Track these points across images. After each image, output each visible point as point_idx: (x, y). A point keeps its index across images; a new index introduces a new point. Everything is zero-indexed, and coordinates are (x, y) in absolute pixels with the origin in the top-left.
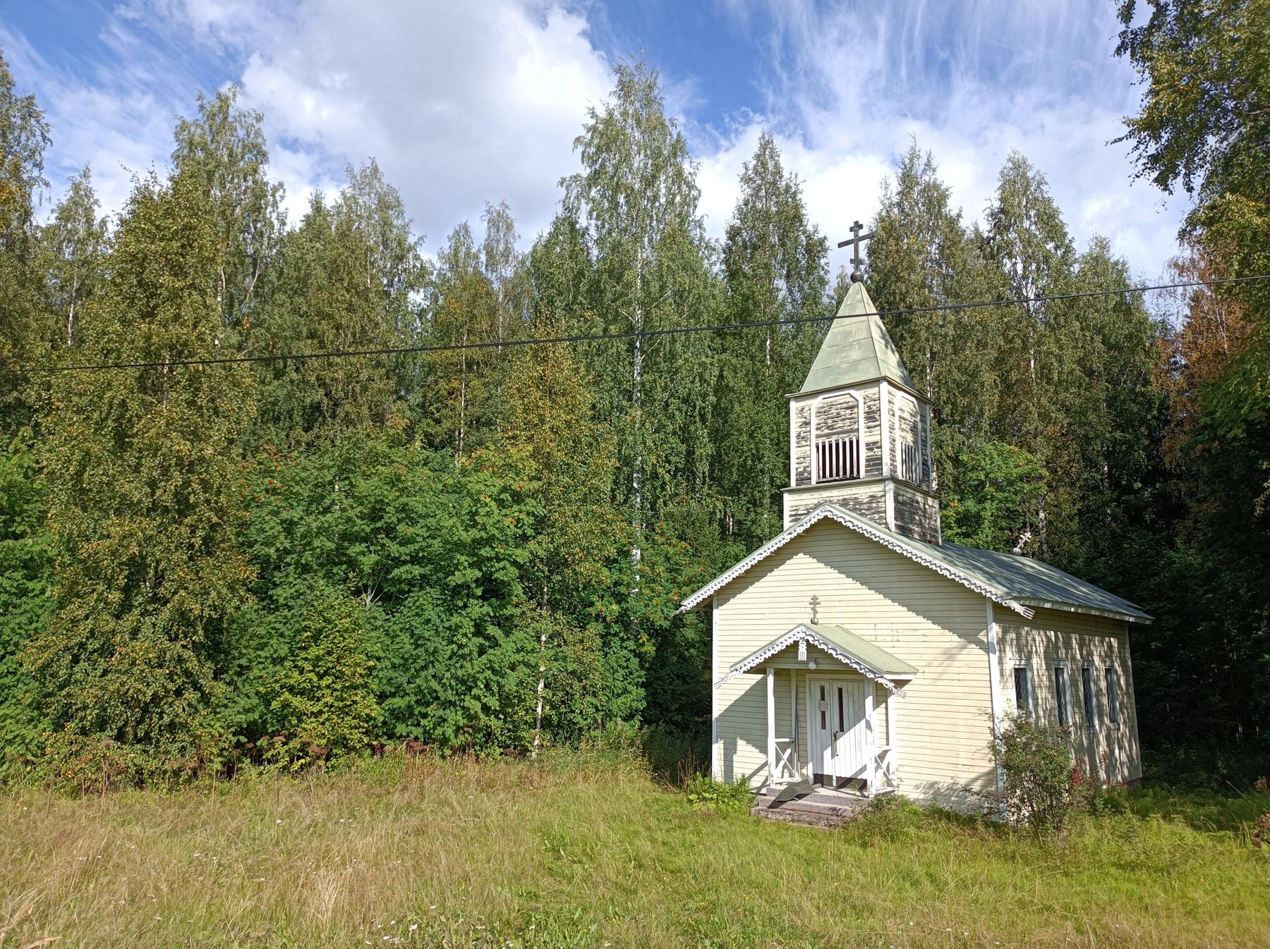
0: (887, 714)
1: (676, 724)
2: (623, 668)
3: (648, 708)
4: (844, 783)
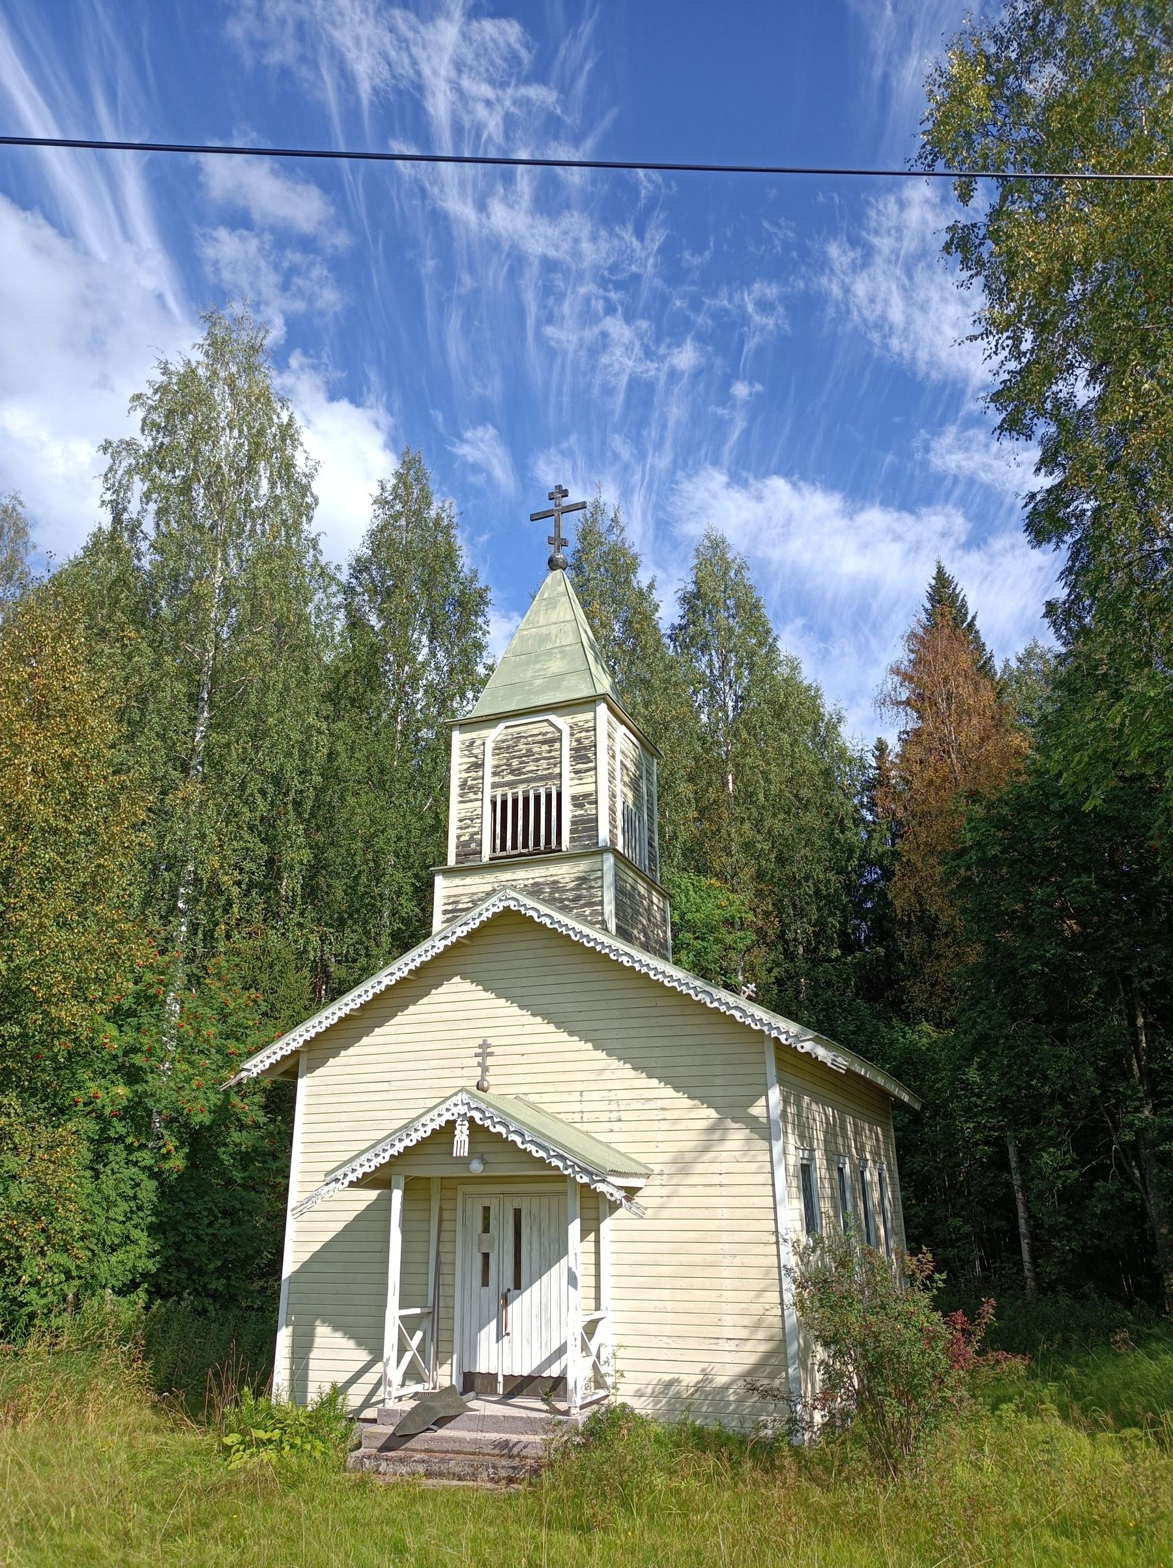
0: (597, 1253)
1: (215, 1296)
2: (127, 1198)
3: (165, 1268)
4: (519, 1386)
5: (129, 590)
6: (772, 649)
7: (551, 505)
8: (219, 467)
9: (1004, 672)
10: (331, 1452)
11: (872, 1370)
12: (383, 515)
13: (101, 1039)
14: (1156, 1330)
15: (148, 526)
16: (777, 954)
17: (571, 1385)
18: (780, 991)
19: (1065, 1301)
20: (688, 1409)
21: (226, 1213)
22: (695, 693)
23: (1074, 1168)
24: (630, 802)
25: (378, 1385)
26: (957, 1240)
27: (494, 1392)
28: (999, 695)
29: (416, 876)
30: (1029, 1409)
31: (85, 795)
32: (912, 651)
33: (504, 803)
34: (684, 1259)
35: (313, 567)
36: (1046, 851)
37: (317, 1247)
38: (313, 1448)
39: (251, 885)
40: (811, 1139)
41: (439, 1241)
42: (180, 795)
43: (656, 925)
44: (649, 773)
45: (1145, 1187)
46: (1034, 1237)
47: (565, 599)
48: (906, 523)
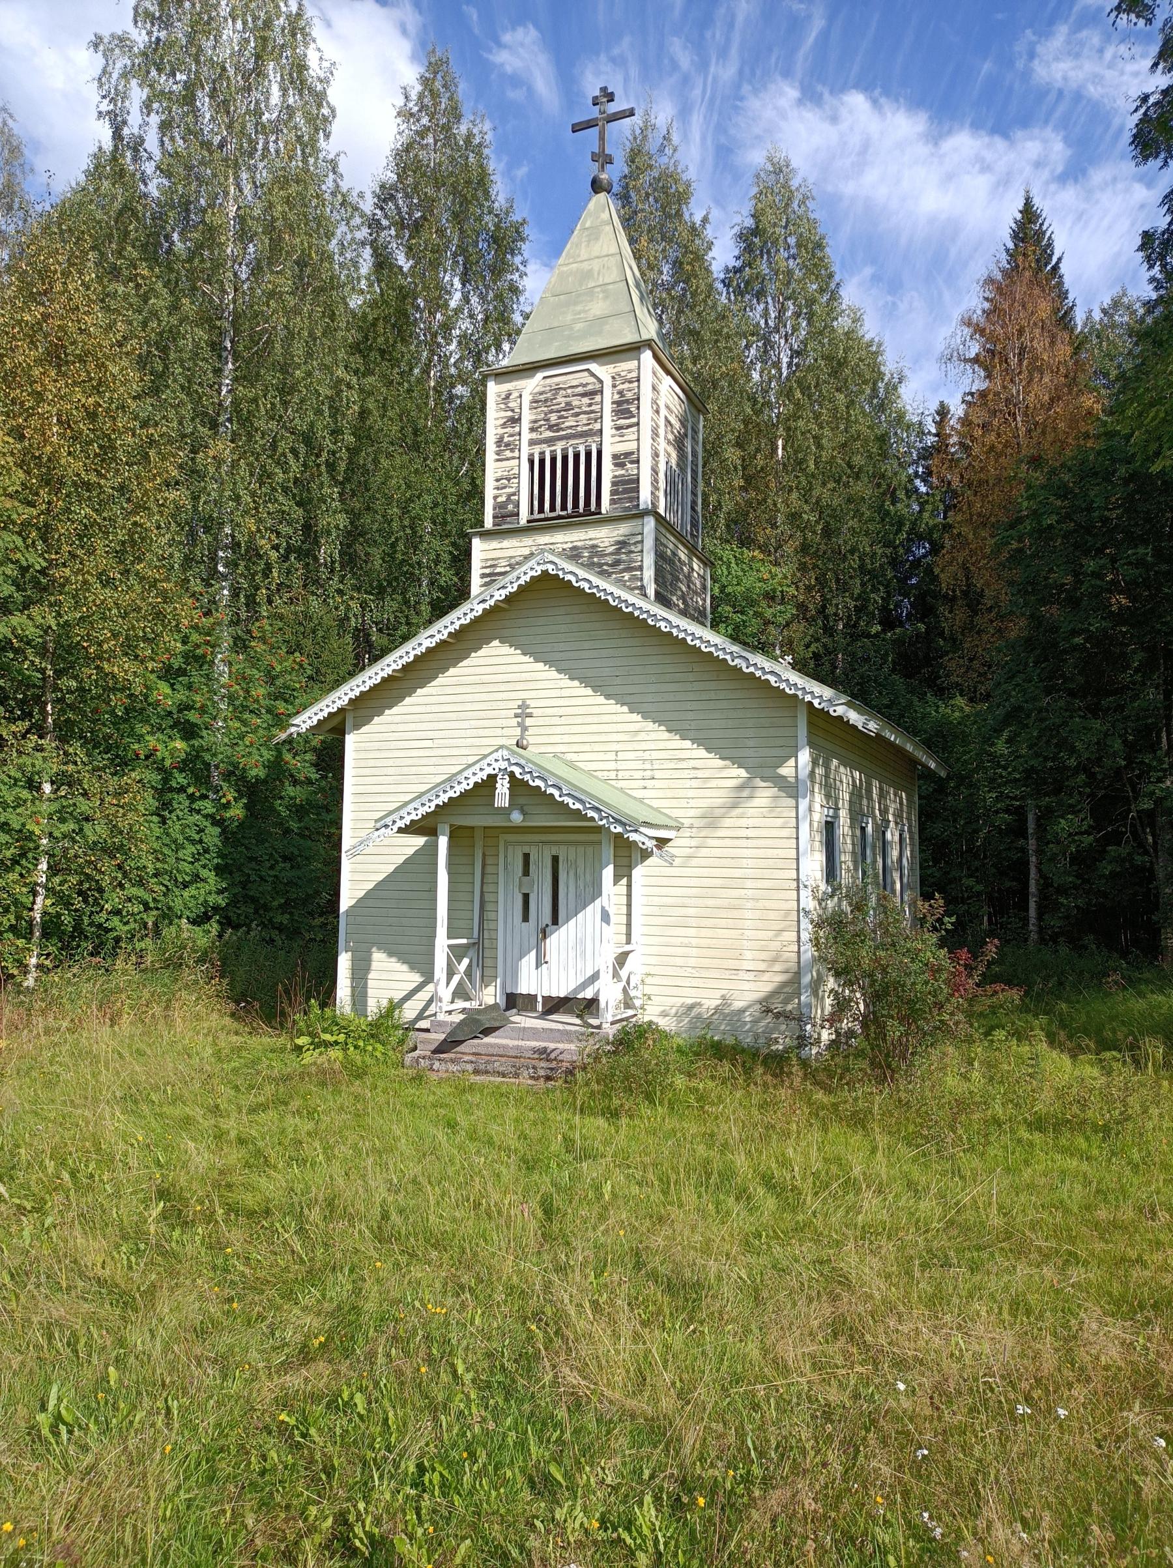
0: (629, 895)
1: (280, 928)
2: (193, 842)
3: (233, 903)
4: (555, 1005)
5: (138, 219)
6: (834, 296)
7: (595, 112)
8: (224, 69)
9: (1085, 325)
10: (391, 1053)
11: (876, 997)
12: (408, 131)
13: (154, 696)
14: (1147, 975)
15: (152, 143)
16: (817, 629)
17: (602, 1005)
18: (817, 666)
19: (1064, 950)
20: (708, 1026)
21: (285, 858)
22: (748, 347)
23: (1089, 834)
24: (673, 462)
25: (430, 1001)
26: (969, 898)
27: (535, 1010)
28: (1077, 350)
29: (454, 544)
30: (1020, 1035)
31: (113, 448)
32: (987, 299)
33: (542, 462)
34: (710, 902)
35: (333, 194)
36: (1105, 520)
37: (371, 886)
38: (374, 1049)
39: (289, 549)
40: (837, 799)
41: (482, 883)
42: (211, 453)
43: (695, 593)
44: (695, 431)
45: (1156, 851)
46: (1043, 897)
47: (609, 228)
48: (998, 151)
